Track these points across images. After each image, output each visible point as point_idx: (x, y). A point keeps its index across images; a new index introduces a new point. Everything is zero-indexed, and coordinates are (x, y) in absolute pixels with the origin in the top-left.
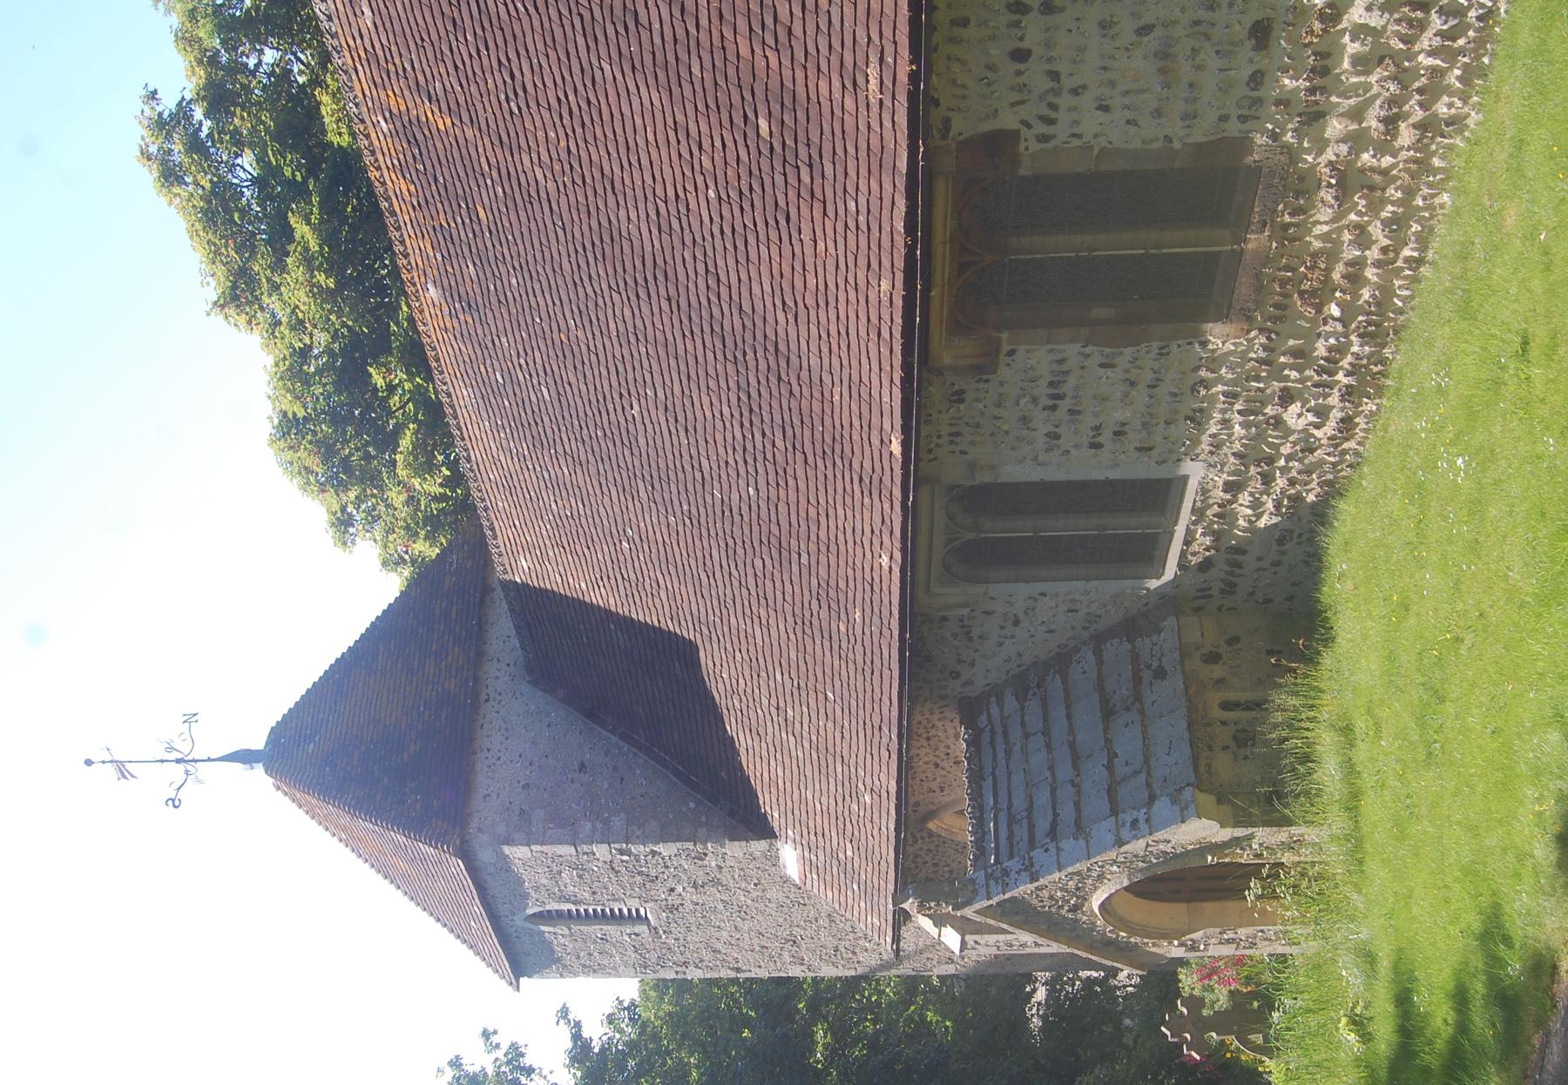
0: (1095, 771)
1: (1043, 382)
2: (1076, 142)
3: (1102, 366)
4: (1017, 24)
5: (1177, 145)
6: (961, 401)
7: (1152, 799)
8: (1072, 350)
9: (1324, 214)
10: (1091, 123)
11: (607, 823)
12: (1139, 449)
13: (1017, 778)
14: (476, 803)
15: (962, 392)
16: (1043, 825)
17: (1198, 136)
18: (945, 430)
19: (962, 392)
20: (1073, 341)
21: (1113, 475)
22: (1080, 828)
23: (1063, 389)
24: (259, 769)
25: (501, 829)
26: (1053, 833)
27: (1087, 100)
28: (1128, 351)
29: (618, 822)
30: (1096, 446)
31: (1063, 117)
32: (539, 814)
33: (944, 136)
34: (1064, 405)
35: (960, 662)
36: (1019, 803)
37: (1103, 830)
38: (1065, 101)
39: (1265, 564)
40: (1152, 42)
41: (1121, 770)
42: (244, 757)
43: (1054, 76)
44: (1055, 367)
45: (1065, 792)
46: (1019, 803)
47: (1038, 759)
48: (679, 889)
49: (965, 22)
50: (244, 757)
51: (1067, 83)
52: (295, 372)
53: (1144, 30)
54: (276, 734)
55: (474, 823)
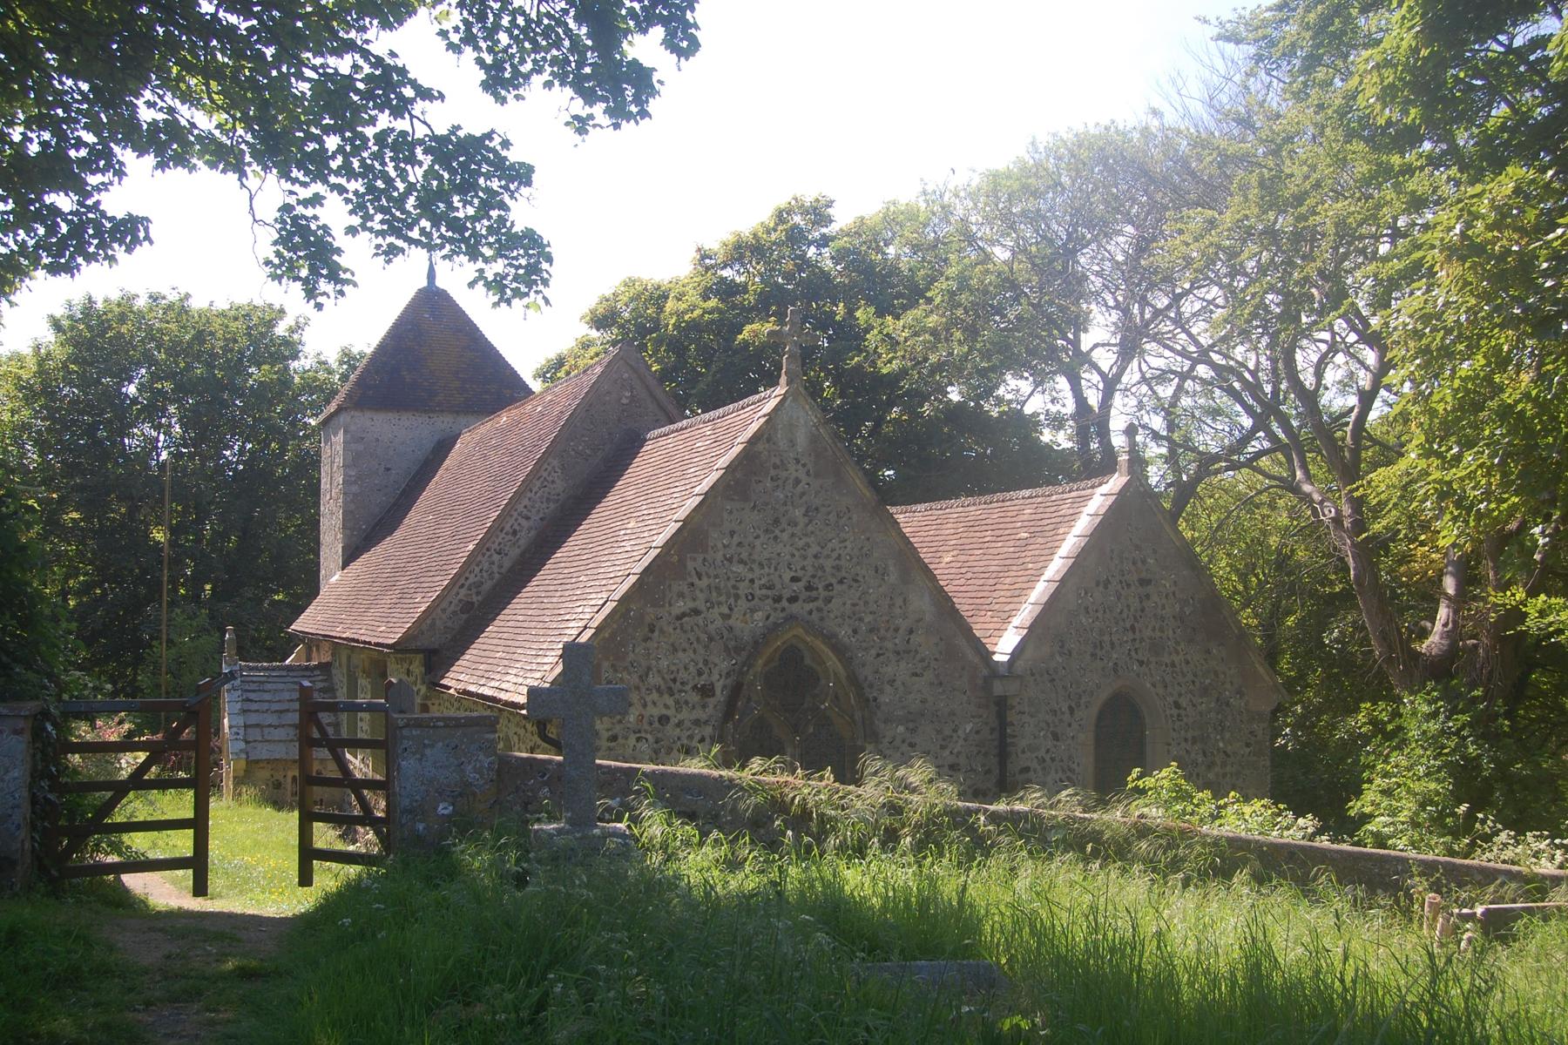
0: (271, 719)
7: (247, 742)
11: (355, 482)
13: (281, 686)
14: (368, 414)
16: (252, 696)
22: (245, 711)
24: (424, 283)
25: (353, 428)
26: (248, 700)
29: (355, 489)
32: (361, 447)
36: (269, 686)
37: (240, 721)
41: (266, 731)
42: (431, 275)
45: (265, 706)
46: (269, 686)
47: (287, 696)
50: (431, 275)
52: (659, 297)
54: (443, 295)
55: (357, 414)
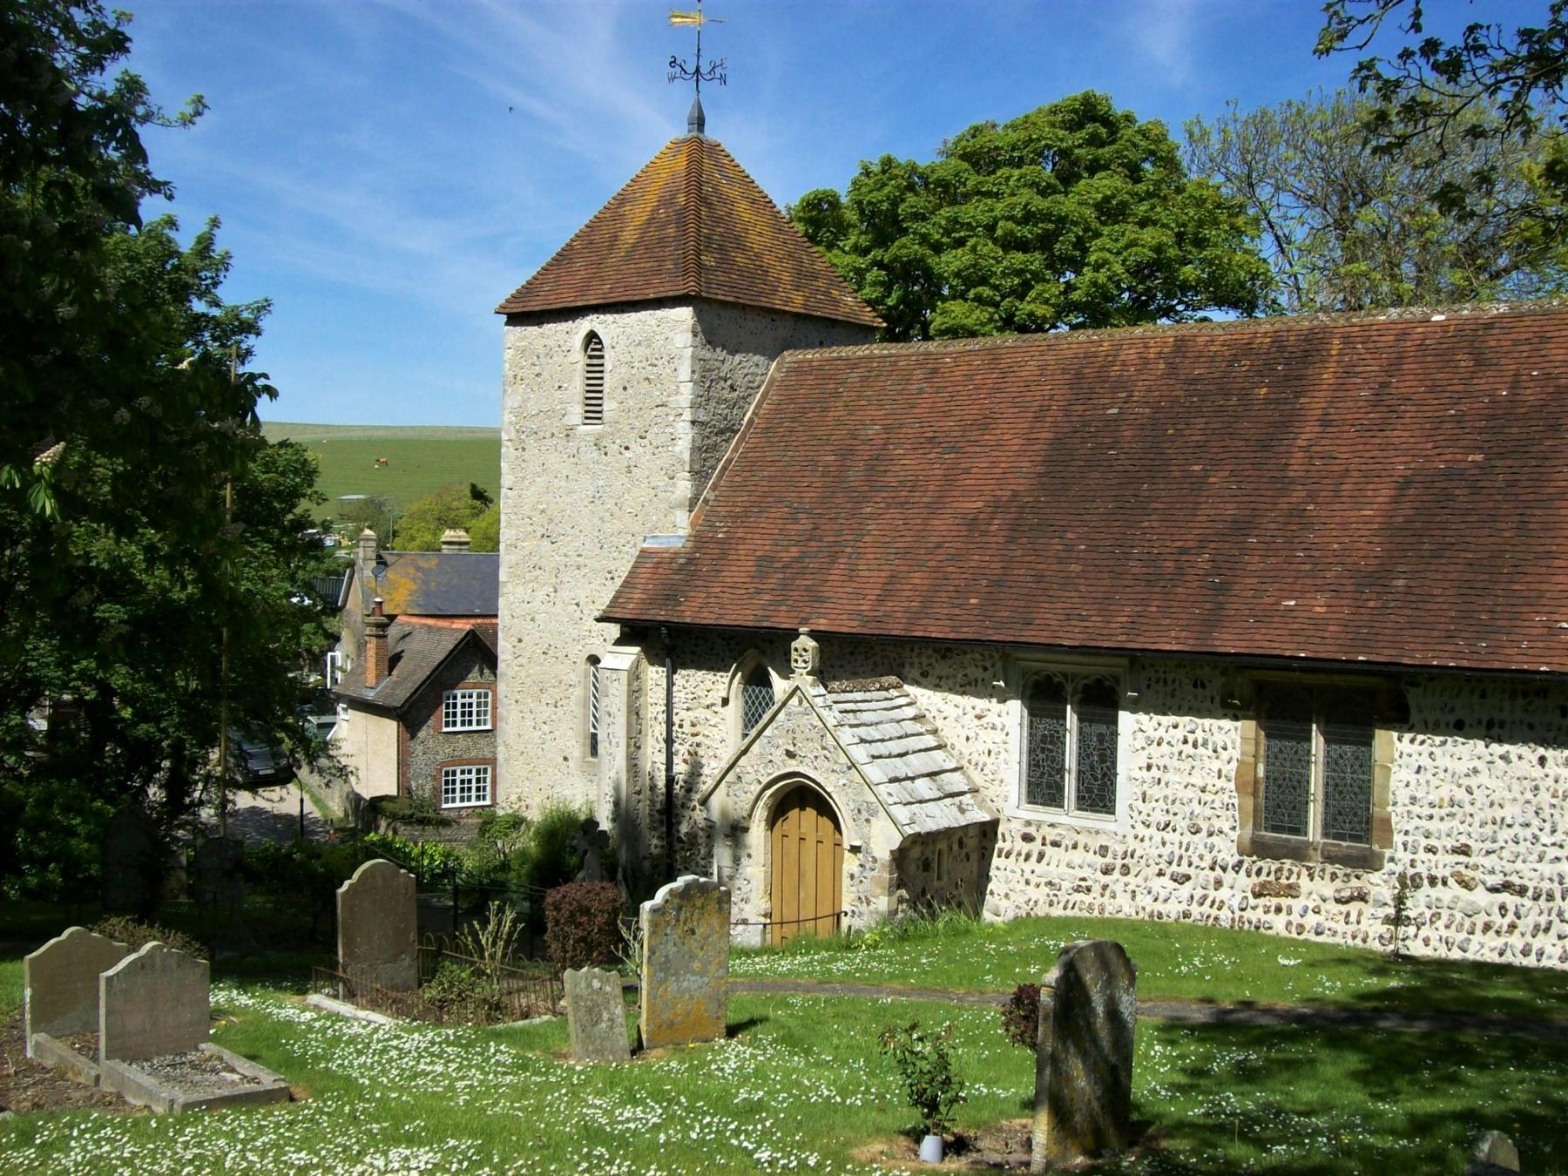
2: (1396, 756)
3: (1220, 771)
4: (1480, 722)
5: (1390, 809)
6: (1195, 686)
8: (1236, 754)
9: (1328, 889)
12: (1144, 794)
15: (1203, 686)
17: (1394, 819)
18: (1170, 677)
19: (1203, 686)
20: (1243, 754)
21: (1121, 780)
23: (1201, 750)
28: (1232, 786)
30: (1149, 767)
33: (1407, 683)
34: (1188, 749)
35: (940, 678)
39: (1028, 875)
40: (1461, 794)
48: (627, 454)
49: (1483, 696)
53: (1469, 791)
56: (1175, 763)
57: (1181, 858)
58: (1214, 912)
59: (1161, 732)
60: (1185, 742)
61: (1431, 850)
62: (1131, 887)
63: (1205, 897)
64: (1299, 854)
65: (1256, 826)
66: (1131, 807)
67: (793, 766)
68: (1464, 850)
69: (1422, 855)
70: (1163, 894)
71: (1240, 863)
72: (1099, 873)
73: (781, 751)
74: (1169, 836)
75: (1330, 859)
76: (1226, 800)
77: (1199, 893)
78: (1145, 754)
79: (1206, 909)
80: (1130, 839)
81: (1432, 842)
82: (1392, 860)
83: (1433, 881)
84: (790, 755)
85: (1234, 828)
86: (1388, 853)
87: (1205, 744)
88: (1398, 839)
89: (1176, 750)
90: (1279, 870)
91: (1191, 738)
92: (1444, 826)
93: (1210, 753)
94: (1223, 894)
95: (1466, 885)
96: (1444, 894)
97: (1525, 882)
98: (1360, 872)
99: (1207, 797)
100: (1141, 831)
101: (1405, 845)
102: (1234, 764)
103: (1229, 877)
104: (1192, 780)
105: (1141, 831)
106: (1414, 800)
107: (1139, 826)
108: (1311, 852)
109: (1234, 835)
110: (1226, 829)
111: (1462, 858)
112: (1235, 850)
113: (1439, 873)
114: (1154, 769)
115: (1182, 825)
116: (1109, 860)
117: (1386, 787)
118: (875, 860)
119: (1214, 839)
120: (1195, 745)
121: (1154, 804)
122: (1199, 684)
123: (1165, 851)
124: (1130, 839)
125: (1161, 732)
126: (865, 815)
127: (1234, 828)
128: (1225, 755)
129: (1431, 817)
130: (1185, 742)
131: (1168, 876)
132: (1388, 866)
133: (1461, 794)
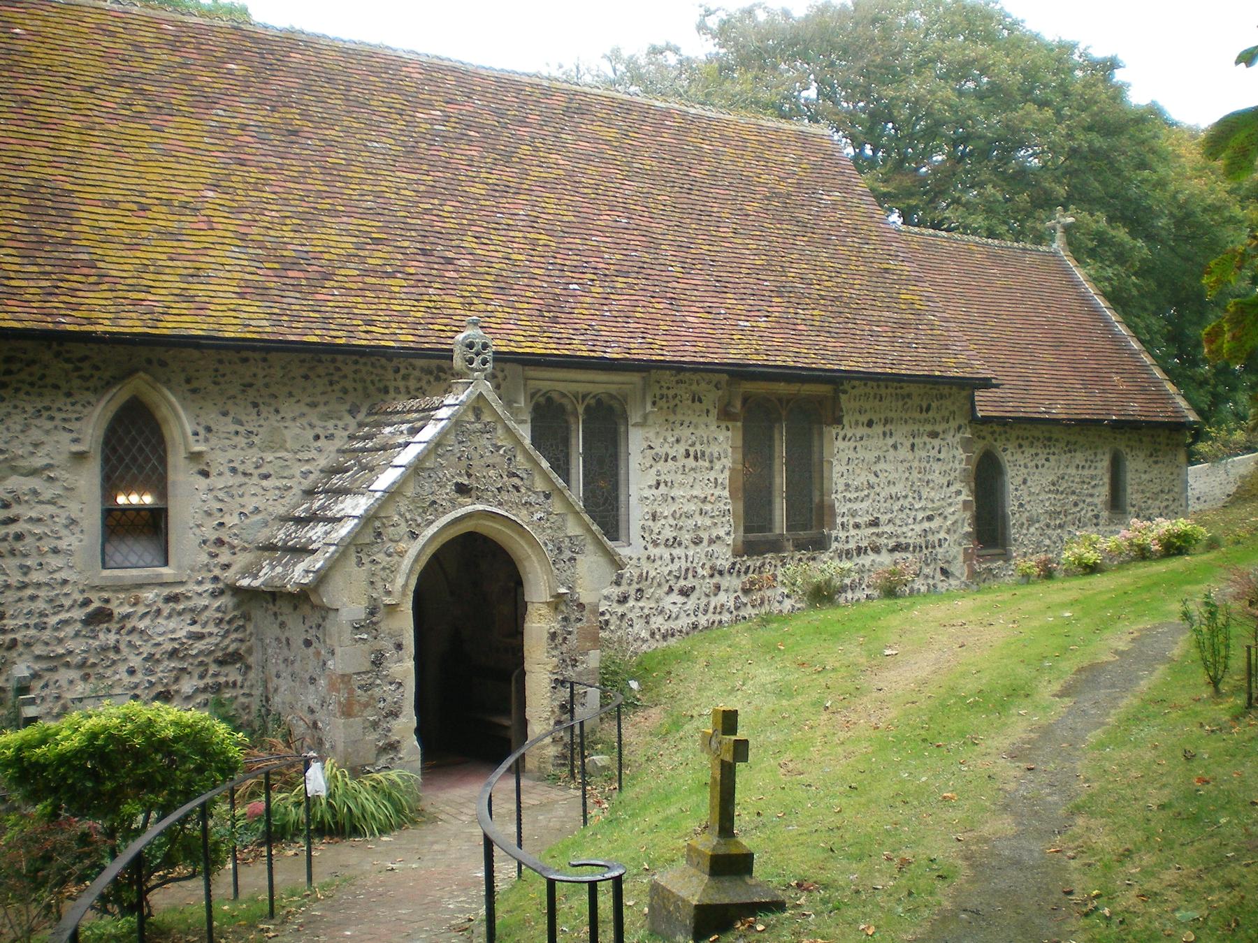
1: (704, 448)
5: (833, 496)
6: (693, 401)
8: (728, 462)
10: (844, 456)
15: (700, 401)
19: (700, 401)
20: (734, 462)
21: (633, 501)
23: (701, 462)
27: (852, 455)
28: (726, 493)
31: (846, 443)
34: (691, 461)
38: (852, 444)
40: (873, 479)
43: (861, 438)
44: (716, 455)
51: (858, 445)
56: (680, 478)
57: (687, 570)
58: (717, 618)
59: (666, 448)
60: (688, 455)
61: (857, 526)
62: (646, 611)
63: (707, 605)
64: (775, 546)
65: (747, 530)
66: (643, 528)
67: (470, 506)
68: (875, 523)
69: (853, 532)
70: (675, 610)
71: (734, 564)
72: (615, 605)
73: (450, 487)
74: (677, 552)
75: (799, 546)
76: (723, 507)
77: (704, 600)
78: (653, 471)
79: (710, 616)
80: (643, 561)
81: (858, 520)
82: (836, 539)
83: (859, 549)
84: (462, 489)
85: (728, 534)
86: (834, 533)
87: (703, 454)
88: (839, 520)
89: (680, 464)
90: (763, 565)
91: (692, 451)
92: (865, 505)
93: (707, 464)
94: (722, 597)
95: (876, 550)
96: (866, 560)
97: (908, 540)
98: (816, 554)
99: (708, 507)
100: (654, 551)
101: (843, 524)
102: (727, 473)
103: (726, 582)
104: (695, 493)
105: (654, 551)
106: (847, 485)
107: (650, 546)
108: (786, 543)
109: (729, 540)
110: (722, 534)
111: (875, 530)
112: (729, 554)
113: (863, 544)
114: (662, 485)
115: (686, 537)
116: (623, 588)
117: (831, 479)
118: (581, 606)
119: (714, 547)
120: (696, 458)
121: (663, 521)
122: (696, 399)
123: (674, 567)
124: (643, 561)
125: (666, 448)
126: (567, 554)
127: (728, 534)
128: (718, 466)
129: (856, 499)
130: (688, 455)
131: (676, 591)
132: (834, 545)
133: (873, 479)
